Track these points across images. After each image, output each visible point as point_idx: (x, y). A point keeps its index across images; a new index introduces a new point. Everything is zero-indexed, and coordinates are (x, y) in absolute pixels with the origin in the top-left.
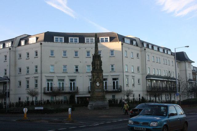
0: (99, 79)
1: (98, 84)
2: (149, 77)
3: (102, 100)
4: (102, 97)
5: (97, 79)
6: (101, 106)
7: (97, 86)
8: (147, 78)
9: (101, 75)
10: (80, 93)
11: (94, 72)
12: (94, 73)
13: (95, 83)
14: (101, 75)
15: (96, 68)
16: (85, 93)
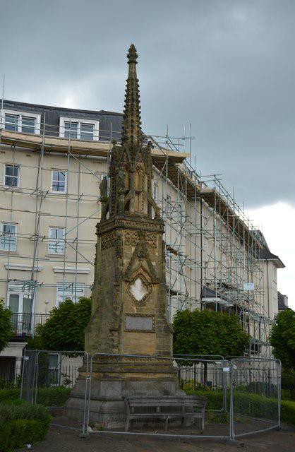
0: (144, 263)
1: (138, 291)
3: (158, 376)
4: (155, 361)
5: (137, 263)
6: (163, 409)
7: (133, 298)
9: (154, 246)
11: (124, 228)
12: (123, 232)
13: (124, 285)
14: (154, 246)
15: (132, 210)
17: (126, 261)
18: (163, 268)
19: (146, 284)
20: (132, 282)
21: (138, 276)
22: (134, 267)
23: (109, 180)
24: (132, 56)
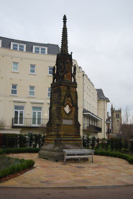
0: (70, 99)
1: (67, 109)
2: (86, 111)
6: (78, 155)
7: (65, 112)
8: (84, 113)
10: (7, 128)
12: (62, 87)
16: (8, 128)
17: (63, 98)
18: (77, 101)
19: (70, 107)
20: (65, 106)
21: (68, 104)
22: (66, 100)
23: (56, 66)
24: (65, 19)
